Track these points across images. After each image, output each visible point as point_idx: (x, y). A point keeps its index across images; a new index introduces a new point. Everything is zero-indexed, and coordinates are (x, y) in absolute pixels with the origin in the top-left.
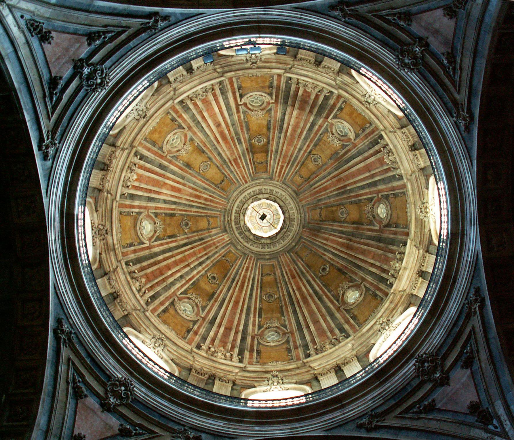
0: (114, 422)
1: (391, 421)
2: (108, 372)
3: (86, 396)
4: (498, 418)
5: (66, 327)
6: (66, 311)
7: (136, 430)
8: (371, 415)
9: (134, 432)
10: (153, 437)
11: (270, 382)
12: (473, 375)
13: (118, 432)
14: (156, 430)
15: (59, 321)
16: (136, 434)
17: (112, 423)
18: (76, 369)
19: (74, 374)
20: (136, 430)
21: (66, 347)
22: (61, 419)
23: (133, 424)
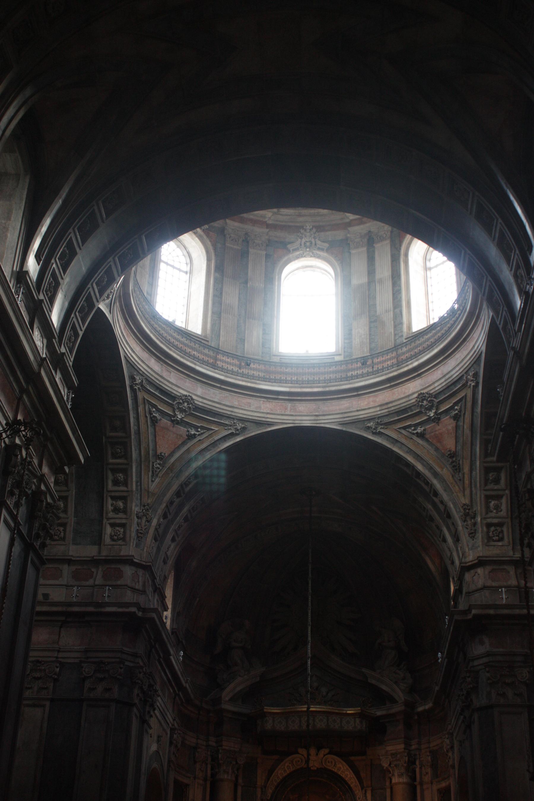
0: (182, 430)
2: (173, 395)
3: (160, 420)
4: (464, 474)
5: (138, 380)
6: (136, 367)
7: (199, 431)
9: (197, 433)
11: (303, 240)
12: (457, 427)
13: (187, 437)
15: (132, 378)
18: (150, 403)
19: (149, 408)
20: (198, 431)
21: (140, 391)
23: (196, 428)
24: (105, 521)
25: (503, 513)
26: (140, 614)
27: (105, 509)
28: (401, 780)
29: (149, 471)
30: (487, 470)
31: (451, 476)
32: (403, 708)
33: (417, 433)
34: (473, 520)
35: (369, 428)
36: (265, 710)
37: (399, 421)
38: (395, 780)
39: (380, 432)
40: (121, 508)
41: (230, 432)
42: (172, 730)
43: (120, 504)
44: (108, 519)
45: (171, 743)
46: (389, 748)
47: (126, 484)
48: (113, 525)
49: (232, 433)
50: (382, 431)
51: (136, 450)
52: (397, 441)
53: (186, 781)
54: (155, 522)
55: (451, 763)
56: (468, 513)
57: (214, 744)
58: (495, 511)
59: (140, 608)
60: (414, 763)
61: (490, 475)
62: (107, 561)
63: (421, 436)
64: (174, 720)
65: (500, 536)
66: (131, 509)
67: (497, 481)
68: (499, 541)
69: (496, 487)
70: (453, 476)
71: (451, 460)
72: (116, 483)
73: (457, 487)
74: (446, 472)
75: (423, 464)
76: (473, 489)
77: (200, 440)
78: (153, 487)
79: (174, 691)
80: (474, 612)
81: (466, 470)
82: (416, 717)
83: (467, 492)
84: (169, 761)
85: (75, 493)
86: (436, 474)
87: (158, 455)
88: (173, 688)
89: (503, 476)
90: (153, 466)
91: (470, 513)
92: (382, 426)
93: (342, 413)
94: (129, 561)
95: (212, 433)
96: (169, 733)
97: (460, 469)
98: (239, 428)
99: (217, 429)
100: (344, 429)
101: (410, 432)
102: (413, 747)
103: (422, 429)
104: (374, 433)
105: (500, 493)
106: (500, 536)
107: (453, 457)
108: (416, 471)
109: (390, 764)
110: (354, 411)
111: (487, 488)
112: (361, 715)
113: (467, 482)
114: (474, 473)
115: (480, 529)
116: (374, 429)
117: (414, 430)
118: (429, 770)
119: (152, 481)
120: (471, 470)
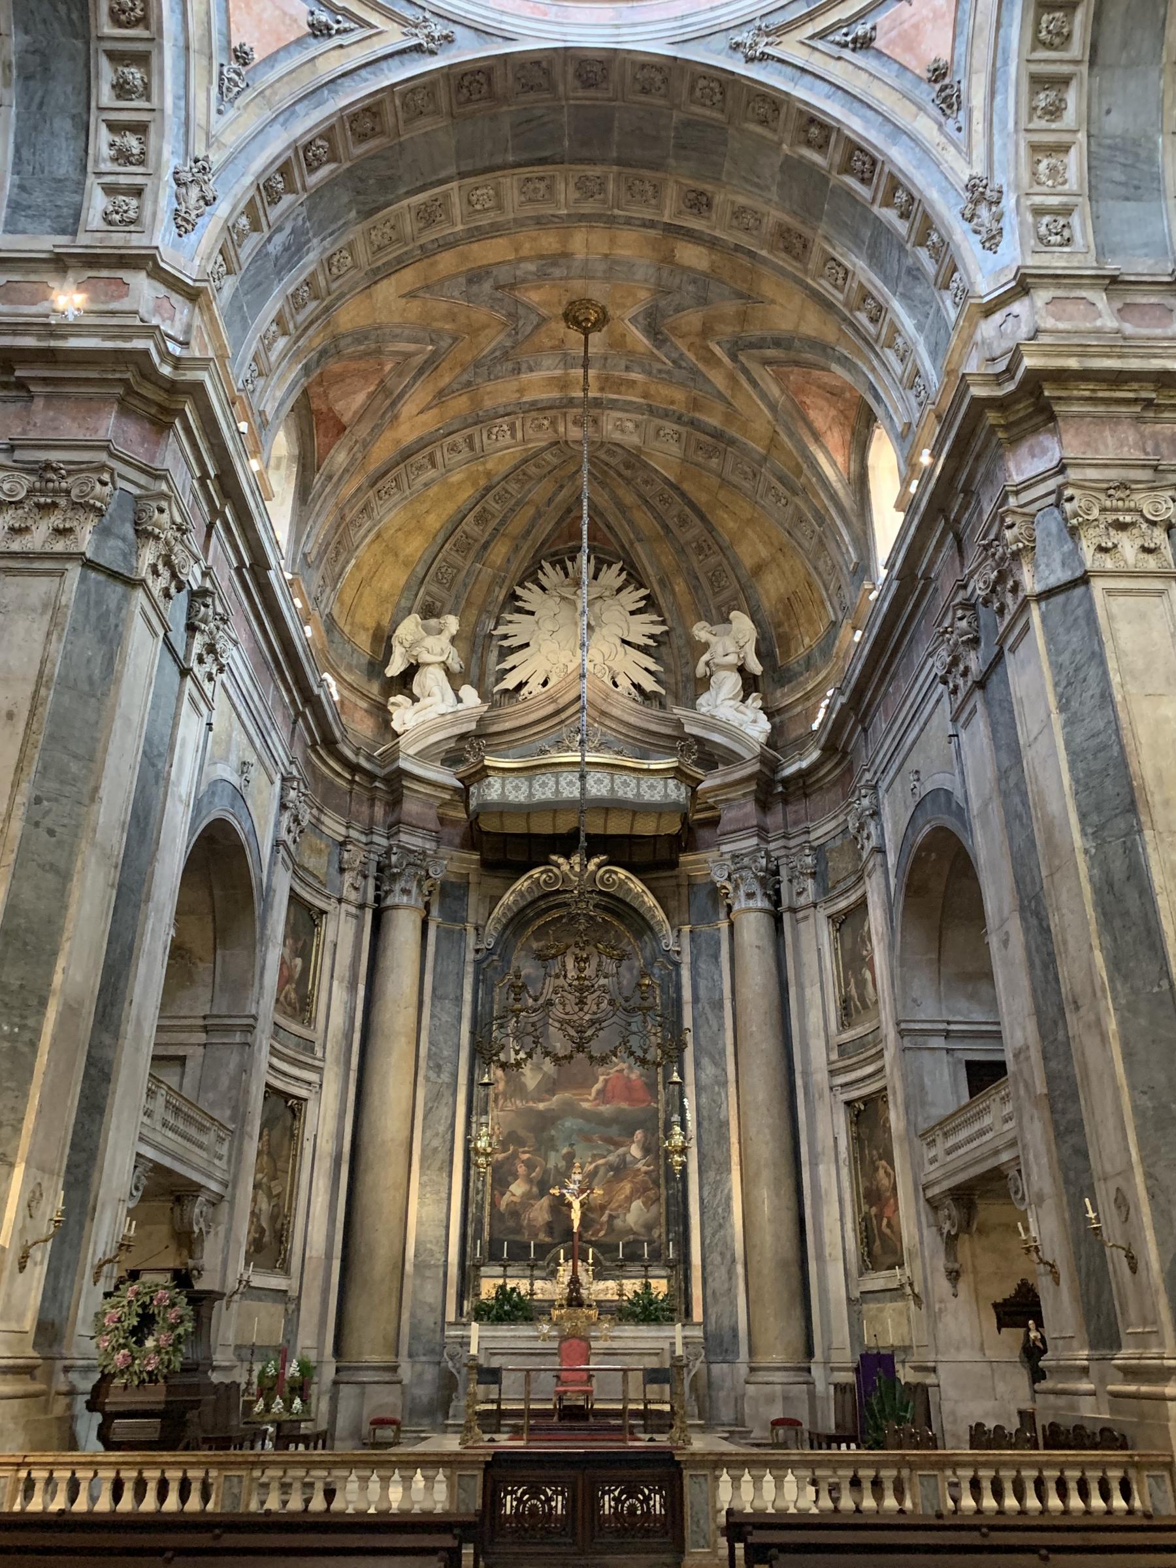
1: (791, 48)
4: (970, 111)
7: (338, 22)
8: (760, 29)
9: (336, 26)
10: (370, 37)
13: (308, 30)
14: (374, 18)
16: (338, 32)
17: (292, 11)
20: (338, 22)
22: (203, 15)
24: (91, 180)
25: (1073, 185)
26: (166, 370)
27: (91, 151)
28: (751, 904)
29: (210, 82)
30: (1039, 82)
31: (936, 127)
32: (757, 767)
33: (855, 41)
34: (994, 209)
35: (736, 47)
36: (486, 763)
37: (810, 16)
38: (740, 904)
39: (763, 53)
40: (135, 151)
41: (414, 41)
42: (284, 779)
43: (132, 142)
44: (99, 174)
45: (283, 807)
46: (724, 848)
47: (146, 94)
48: (110, 190)
49: (420, 45)
50: (768, 50)
51: (173, 11)
52: (803, 70)
53: (320, 903)
54: (222, 209)
55: (873, 842)
56: (983, 193)
57: (384, 842)
58: (1050, 183)
59: (165, 355)
60: (776, 872)
61: (1042, 96)
62: (91, 261)
63: (863, 44)
64: (291, 763)
65: (1066, 234)
66: (159, 153)
67: (1055, 111)
68: (1061, 245)
69: (1054, 126)
70: (940, 126)
71: (938, 87)
72: (122, 89)
73: (952, 149)
74: (925, 126)
75: (863, 118)
76: (996, 138)
77: (341, 46)
78: (218, 124)
79: (293, 701)
80: (1028, 362)
81: (977, 97)
82: (780, 789)
83: (979, 152)
84: (277, 843)
85: (18, 115)
86: (898, 131)
87: (235, 50)
88: (289, 690)
89: (1072, 97)
90: (221, 73)
91: (988, 192)
92: (770, 39)
93: (676, 19)
94: (147, 262)
95: (370, 37)
96: (278, 783)
97: (959, 103)
98: (436, 35)
99: (382, 28)
100: (680, 55)
101: (838, 44)
102: (772, 846)
103: (868, 26)
104: (750, 60)
105: (1066, 138)
106: (1066, 234)
107: (944, 75)
108: (849, 140)
109: (729, 878)
110: (705, 11)
111: (1031, 126)
112: (678, 773)
113: (978, 127)
114: (998, 99)
115: (1015, 221)
116: (751, 47)
117: (846, 35)
118: (810, 884)
119: (220, 112)
120: (992, 94)
